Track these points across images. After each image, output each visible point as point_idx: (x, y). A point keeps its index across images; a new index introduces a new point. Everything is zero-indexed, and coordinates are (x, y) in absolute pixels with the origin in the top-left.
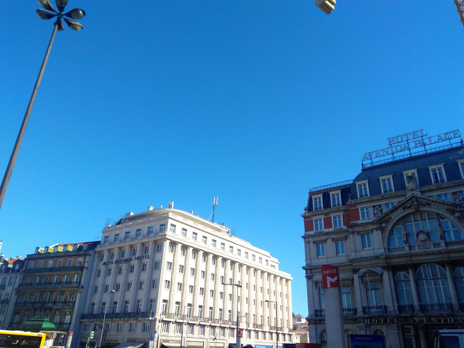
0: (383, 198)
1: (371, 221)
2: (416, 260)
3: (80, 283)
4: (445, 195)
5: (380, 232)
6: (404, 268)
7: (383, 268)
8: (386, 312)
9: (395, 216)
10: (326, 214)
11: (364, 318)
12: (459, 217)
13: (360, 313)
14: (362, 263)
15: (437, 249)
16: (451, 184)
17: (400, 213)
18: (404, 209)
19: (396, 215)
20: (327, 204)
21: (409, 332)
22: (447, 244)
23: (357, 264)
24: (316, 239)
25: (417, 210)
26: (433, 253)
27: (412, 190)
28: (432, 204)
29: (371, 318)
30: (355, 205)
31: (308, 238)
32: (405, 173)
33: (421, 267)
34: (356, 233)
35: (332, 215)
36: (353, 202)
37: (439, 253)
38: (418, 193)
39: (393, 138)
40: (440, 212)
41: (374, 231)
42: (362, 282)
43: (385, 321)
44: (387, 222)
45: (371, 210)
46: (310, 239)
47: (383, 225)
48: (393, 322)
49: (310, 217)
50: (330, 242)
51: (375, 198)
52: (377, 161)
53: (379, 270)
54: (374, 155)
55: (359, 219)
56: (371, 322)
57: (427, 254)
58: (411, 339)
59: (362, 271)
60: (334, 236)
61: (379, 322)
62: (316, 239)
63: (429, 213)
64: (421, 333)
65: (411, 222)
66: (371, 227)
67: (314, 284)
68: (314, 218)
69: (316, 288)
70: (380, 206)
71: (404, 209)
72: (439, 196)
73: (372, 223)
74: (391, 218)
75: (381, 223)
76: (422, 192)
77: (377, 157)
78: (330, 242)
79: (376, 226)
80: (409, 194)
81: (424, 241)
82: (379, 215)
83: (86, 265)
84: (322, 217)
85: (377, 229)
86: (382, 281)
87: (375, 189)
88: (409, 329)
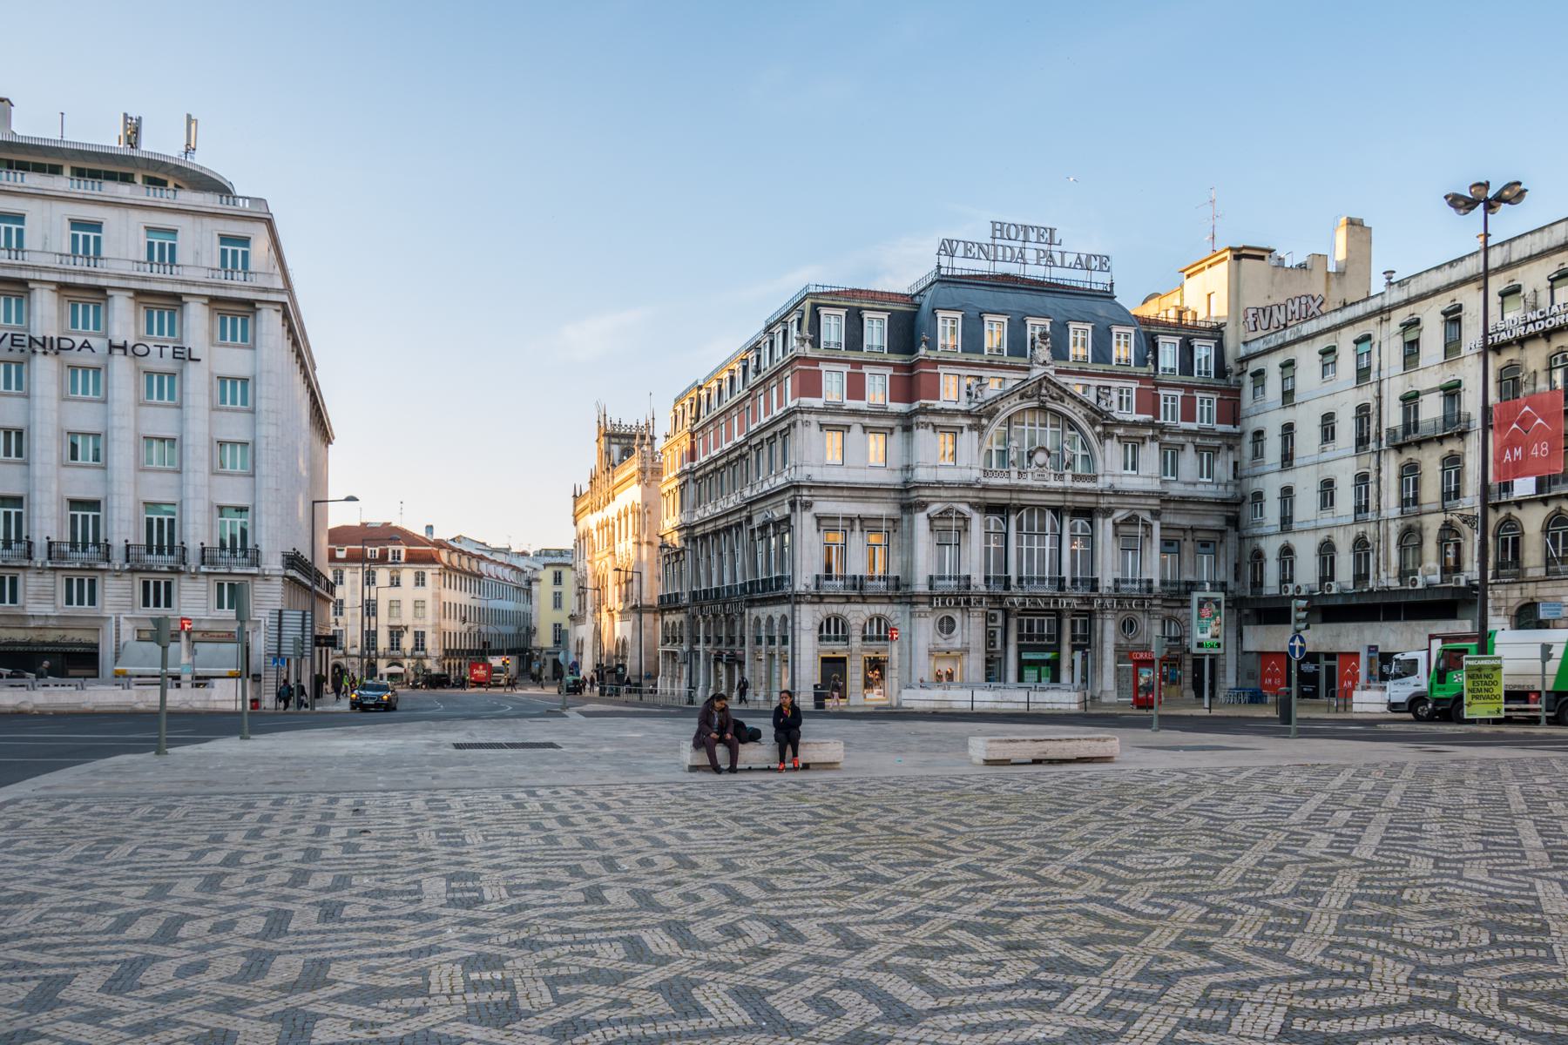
0: (990, 365)
1: (963, 406)
5: (976, 434)
7: (972, 505)
8: (968, 587)
9: (1008, 408)
10: (857, 364)
11: (931, 596)
12: (1098, 434)
13: (921, 586)
14: (937, 492)
15: (1059, 484)
16: (1101, 368)
18: (1021, 398)
19: (1007, 406)
20: (855, 338)
21: (995, 621)
22: (1075, 477)
23: (927, 492)
24: (826, 419)
25: (1042, 408)
26: (1055, 492)
27: (1045, 363)
28: (1067, 399)
29: (943, 596)
30: (936, 363)
31: (810, 412)
32: (1030, 321)
33: (1024, 511)
34: (930, 427)
35: (866, 370)
36: (933, 355)
37: (1064, 492)
39: (1002, 224)
40: (1075, 418)
41: (965, 430)
42: (932, 530)
43: (968, 602)
44: (991, 415)
46: (813, 418)
47: (984, 421)
48: (981, 602)
49: (816, 361)
50: (856, 431)
51: (976, 358)
52: (963, 265)
53: (964, 508)
54: (960, 251)
55: (938, 398)
56: (943, 603)
58: (994, 632)
59: (935, 508)
60: (867, 421)
61: (958, 603)
62: (826, 419)
64: (1013, 623)
65: (1023, 424)
66: (964, 422)
67: (815, 521)
68: (823, 367)
69: (819, 530)
71: (1021, 398)
73: (967, 414)
74: (998, 410)
75: (980, 417)
76: (1057, 372)
77: (965, 257)
78: (856, 431)
79: (969, 422)
80: (1037, 372)
81: (1041, 466)
82: (980, 400)
84: (846, 369)
85: (971, 428)
86: (966, 530)
87: (973, 340)
88: (995, 615)
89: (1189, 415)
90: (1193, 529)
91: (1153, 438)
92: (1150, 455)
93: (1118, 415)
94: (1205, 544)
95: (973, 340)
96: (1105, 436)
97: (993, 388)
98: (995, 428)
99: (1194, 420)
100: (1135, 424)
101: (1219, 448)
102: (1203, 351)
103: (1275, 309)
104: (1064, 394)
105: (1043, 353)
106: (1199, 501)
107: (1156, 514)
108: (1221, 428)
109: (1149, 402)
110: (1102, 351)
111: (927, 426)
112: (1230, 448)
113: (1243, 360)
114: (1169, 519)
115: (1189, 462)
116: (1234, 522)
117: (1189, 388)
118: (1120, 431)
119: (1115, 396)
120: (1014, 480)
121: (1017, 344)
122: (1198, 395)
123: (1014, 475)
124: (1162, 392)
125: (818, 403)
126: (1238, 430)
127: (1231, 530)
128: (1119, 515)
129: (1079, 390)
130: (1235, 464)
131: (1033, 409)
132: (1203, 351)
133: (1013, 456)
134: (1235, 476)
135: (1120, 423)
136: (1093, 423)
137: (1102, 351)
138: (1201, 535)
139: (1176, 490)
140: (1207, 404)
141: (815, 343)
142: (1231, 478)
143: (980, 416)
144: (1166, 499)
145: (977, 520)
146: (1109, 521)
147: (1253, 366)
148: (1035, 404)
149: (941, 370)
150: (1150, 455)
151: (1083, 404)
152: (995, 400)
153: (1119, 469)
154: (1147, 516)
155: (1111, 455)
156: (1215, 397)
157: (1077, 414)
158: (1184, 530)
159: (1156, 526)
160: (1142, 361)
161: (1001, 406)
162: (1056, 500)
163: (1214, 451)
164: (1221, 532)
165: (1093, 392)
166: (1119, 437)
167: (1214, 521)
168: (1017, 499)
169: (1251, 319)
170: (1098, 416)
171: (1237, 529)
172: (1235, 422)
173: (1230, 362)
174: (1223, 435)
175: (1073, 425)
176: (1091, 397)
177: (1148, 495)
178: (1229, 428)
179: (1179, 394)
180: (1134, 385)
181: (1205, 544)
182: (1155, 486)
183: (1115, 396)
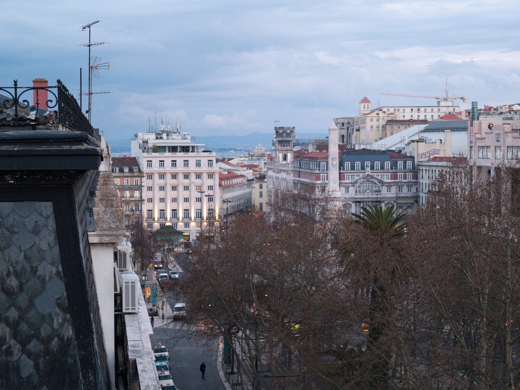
1: (350, 181)
2: (364, 200)
3: (141, 197)
4: (378, 176)
6: (359, 202)
7: (352, 202)
9: (360, 182)
15: (372, 196)
16: (382, 171)
17: (362, 180)
25: (368, 181)
26: (371, 198)
36: (344, 172)
37: (373, 198)
38: (370, 174)
44: (356, 183)
45: (350, 177)
49: (320, 174)
53: (350, 203)
57: (368, 198)
63: (371, 181)
68: (321, 175)
70: (354, 175)
72: (376, 175)
73: (351, 183)
80: (367, 173)
83: (143, 184)
85: (352, 186)
87: (353, 168)
89: (405, 178)
90: (406, 204)
91: (394, 185)
92: (394, 189)
93: (385, 180)
94: (409, 207)
95: (353, 168)
96: (382, 186)
97: (356, 178)
98: (357, 185)
99: (406, 179)
100: (390, 183)
101: (412, 185)
102: (409, 163)
103: (427, 153)
104: (372, 177)
105: (369, 169)
106: (407, 197)
107: (395, 202)
108: (413, 181)
109: (394, 177)
110: (382, 168)
111: (342, 186)
112: (416, 185)
113: (418, 165)
114: (400, 201)
115: (405, 189)
116: (417, 201)
117: (405, 172)
118: (386, 184)
119: (385, 177)
120: (362, 196)
121: (363, 168)
122: (407, 174)
123: (362, 195)
124: (398, 174)
125: (320, 182)
126: (418, 181)
127: (416, 203)
128: (386, 202)
129: (375, 176)
130: (417, 189)
131: (366, 181)
132: (409, 163)
133: (362, 191)
134: (417, 191)
135: (386, 183)
136: (380, 183)
137: (382, 168)
138: (408, 205)
139: (402, 195)
140: (409, 176)
141: (319, 170)
142: (416, 192)
143: (353, 184)
144: (398, 198)
145: (353, 205)
146: (384, 204)
147: (421, 168)
148: (366, 180)
149: (346, 174)
150: (394, 189)
151: (377, 179)
152: (357, 180)
153: (386, 192)
154: (392, 202)
155: (384, 189)
156: (412, 174)
157: (376, 182)
158: (404, 204)
159: (395, 204)
160: (392, 168)
161: (359, 181)
162: (372, 200)
163: (411, 186)
164: (413, 204)
165: (380, 176)
166: (386, 186)
167: (412, 201)
168: (362, 200)
169: (420, 156)
170: (381, 182)
171: (417, 203)
172: (417, 179)
173: (416, 165)
174: (414, 182)
175: (375, 184)
176: (379, 178)
177: (392, 198)
178: (415, 180)
179: (403, 174)
180: (390, 174)
181: (409, 207)
182: (395, 196)
183: (385, 177)
